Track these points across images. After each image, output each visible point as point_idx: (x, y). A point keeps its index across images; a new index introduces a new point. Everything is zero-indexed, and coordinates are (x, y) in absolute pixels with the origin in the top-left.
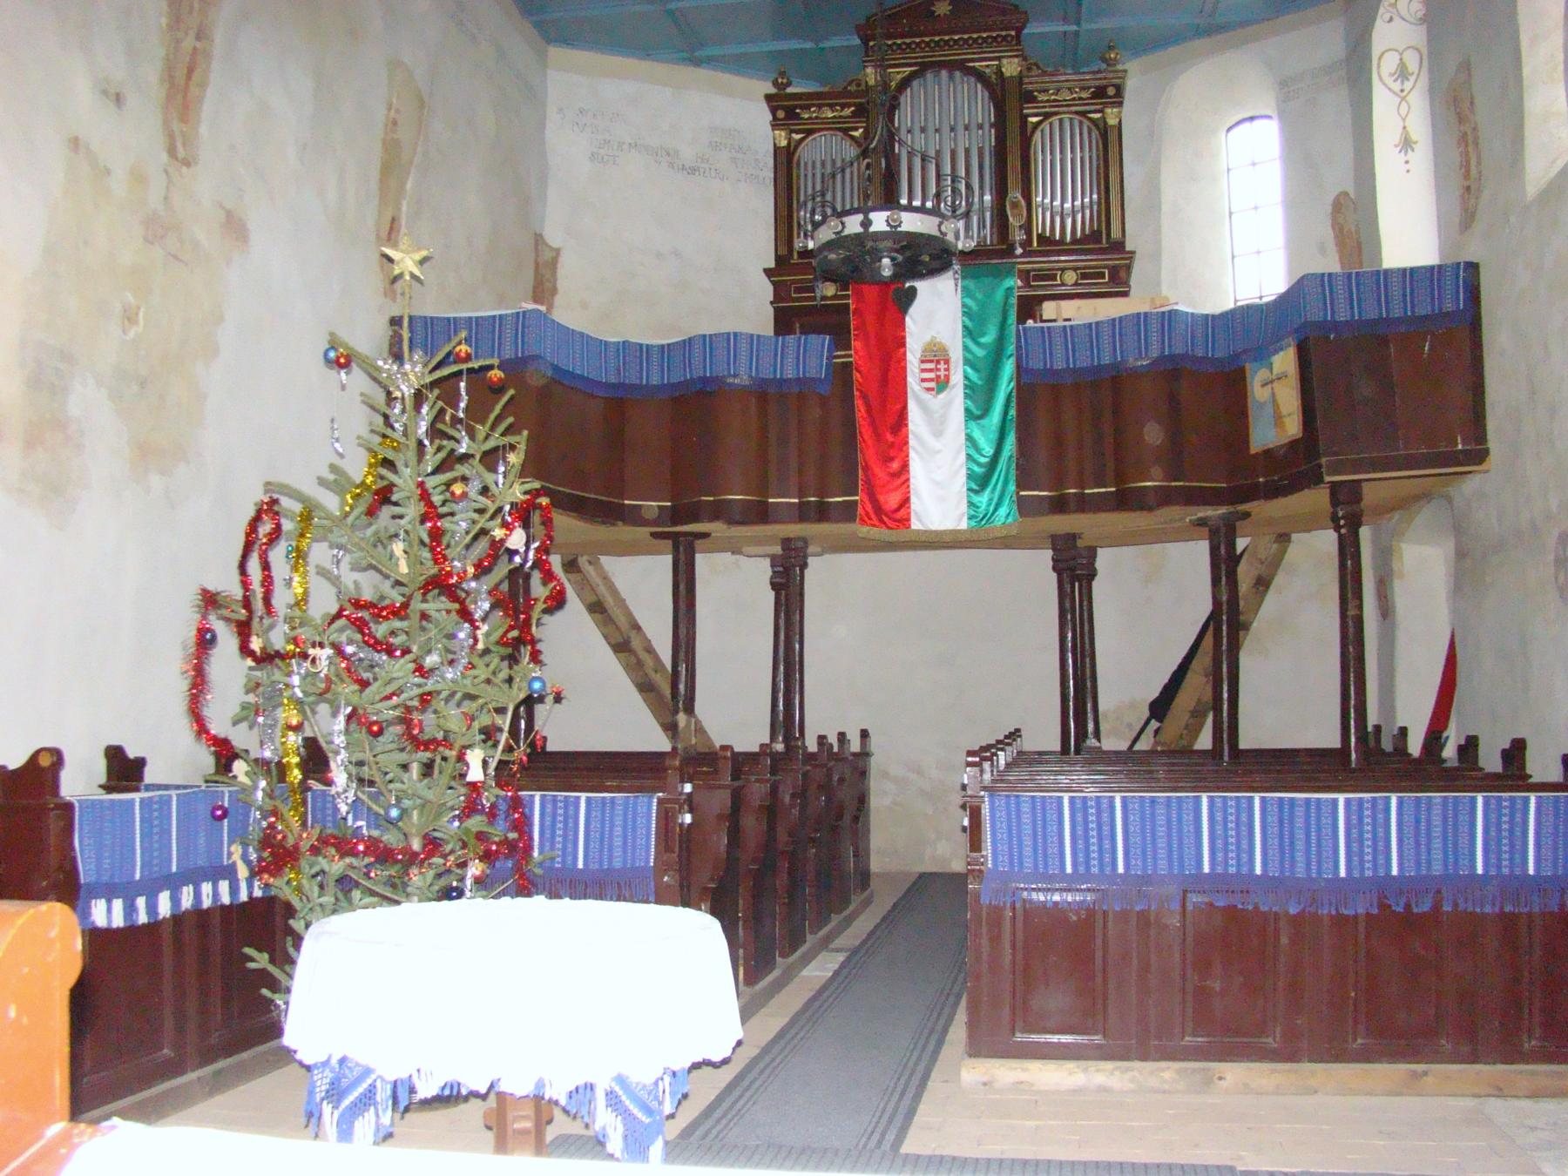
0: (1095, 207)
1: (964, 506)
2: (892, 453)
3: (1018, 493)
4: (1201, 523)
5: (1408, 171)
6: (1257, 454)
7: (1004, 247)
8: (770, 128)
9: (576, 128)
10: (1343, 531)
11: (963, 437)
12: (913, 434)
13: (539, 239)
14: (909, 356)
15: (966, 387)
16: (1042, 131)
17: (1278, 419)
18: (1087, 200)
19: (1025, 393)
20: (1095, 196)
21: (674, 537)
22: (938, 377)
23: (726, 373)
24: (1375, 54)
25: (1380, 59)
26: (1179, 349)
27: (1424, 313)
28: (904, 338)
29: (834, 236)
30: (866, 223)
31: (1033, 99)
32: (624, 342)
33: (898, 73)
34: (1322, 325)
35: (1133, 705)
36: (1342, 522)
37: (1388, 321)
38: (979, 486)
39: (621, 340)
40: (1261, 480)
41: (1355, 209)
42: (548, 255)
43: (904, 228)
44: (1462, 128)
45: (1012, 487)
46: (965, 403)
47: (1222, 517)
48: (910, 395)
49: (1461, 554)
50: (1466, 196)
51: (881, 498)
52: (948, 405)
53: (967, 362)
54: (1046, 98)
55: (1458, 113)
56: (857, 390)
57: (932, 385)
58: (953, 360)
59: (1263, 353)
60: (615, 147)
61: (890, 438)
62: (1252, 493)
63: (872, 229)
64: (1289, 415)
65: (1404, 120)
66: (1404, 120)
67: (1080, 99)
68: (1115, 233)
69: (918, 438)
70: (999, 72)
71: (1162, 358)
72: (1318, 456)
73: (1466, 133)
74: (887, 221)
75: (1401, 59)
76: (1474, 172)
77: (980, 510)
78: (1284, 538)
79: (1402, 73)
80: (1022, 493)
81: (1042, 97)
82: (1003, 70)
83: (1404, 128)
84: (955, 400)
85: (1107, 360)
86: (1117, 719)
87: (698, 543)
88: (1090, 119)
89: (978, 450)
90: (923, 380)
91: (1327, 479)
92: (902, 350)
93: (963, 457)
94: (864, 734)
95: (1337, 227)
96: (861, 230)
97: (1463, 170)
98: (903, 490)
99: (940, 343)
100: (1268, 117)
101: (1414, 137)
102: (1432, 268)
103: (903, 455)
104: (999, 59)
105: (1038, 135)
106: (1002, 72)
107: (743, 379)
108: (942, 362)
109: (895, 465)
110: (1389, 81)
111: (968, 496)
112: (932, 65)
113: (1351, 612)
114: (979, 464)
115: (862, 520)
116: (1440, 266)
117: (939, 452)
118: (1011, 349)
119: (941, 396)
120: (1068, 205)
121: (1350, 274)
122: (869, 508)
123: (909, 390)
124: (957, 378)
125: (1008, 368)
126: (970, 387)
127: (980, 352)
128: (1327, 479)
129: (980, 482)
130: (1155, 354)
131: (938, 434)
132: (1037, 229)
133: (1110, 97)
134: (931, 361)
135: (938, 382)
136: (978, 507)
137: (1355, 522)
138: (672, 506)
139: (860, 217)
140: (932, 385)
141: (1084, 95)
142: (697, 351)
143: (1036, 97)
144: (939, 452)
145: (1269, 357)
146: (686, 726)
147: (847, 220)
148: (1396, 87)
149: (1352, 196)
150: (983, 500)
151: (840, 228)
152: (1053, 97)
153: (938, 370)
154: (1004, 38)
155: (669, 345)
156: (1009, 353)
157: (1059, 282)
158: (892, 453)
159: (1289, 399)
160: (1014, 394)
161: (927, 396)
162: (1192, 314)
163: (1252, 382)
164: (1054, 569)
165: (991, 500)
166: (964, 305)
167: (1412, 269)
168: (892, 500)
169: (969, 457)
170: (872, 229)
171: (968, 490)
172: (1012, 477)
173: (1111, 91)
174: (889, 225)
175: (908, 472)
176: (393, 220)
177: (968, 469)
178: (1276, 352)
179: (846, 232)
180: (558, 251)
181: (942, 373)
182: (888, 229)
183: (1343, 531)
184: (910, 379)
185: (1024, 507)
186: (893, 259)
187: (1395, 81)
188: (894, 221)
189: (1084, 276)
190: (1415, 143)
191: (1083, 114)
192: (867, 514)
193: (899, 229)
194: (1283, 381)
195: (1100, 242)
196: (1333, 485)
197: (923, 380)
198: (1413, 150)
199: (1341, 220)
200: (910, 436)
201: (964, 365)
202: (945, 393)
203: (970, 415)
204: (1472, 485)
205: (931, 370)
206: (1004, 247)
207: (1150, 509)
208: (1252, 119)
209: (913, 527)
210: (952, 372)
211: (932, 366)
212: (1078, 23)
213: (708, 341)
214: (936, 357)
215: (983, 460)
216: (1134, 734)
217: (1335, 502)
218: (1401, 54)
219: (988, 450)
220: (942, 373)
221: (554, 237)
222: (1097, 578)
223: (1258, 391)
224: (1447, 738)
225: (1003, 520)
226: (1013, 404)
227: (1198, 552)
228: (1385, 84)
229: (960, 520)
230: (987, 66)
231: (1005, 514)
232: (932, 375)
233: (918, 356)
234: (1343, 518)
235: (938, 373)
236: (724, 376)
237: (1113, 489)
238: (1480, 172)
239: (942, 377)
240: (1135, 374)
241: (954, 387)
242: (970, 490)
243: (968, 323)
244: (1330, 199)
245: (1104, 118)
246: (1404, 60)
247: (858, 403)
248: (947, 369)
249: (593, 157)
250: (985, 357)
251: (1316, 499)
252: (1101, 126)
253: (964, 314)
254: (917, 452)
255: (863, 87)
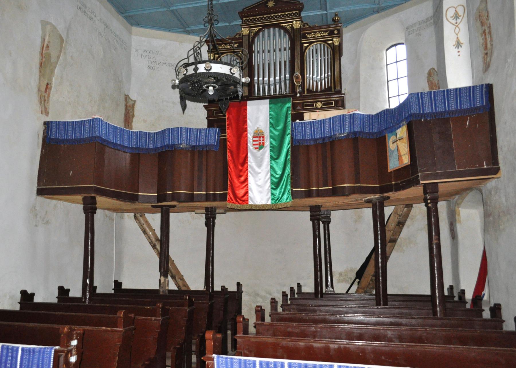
0: (330, 78)
1: (270, 195)
2: (241, 174)
3: (292, 190)
4: (369, 201)
5: (459, 55)
6: (391, 172)
7: (294, 94)
8: (207, 53)
9: (142, 56)
10: (430, 205)
11: (269, 167)
12: (250, 166)
13: (127, 97)
14: (249, 135)
15: (271, 147)
16: (309, 49)
17: (400, 156)
18: (326, 75)
19: (295, 148)
20: (329, 73)
21: (161, 207)
22: (260, 143)
23: (177, 143)
24: (445, 8)
25: (447, 11)
26: (357, 129)
27: (466, 107)
28: (247, 128)
29: (183, 76)
30: (196, 69)
31: (306, 37)
32: (140, 132)
33: (254, 30)
34: (420, 115)
35: (351, 270)
36: (429, 201)
37: (449, 112)
38: (275, 186)
39: (139, 131)
40: (393, 183)
41: (437, 75)
42: (131, 103)
43: (213, 71)
44: (483, 28)
45: (289, 187)
46: (270, 153)
47: (377, 199)
48: (248, 151)
49: (487, 215)
50: (486, 57)
51: (237, 192)
52: (263, 155)
53: (271, 137)
54: (310, 36)
55: (482, 22)
56: (228, 149)
57: (257, 146)
58: (265, 137)
59: (393, 129)
60: (157, 64)
61: (240, 168)
62: (389, 189)
63: (198, 72)
64: (404, 155)
65: (457, 35)
66: (457, 35)
67: (324, 36)
68: (338, 87)
69: (252, 168)
70: (292, 27)
71: (350, 134)
72: (418, 173)
73: (485, 30)
74: (205, 68)
75: (456, 10)
76: (489, 45)
77: (276, 196)
78: (409, 206)
79: (456, 16)
80: (294, 189)
81: (309, 36)
82: (294, 26)
83: (457, 38)
84: (267, 152)
85: (327, 135)
86: (346, 275)
87: (171, 210)
88: (328, 44)
89: (276, 172)
90: (254, 145)
91: (422, 182)
92: (246, 133)
93: (269, 175)
94: (239, 285)
95: (429, 82)
96: (194, 72)
97: (484, 45)
98: (245, 189)
99: (261, 130)
100: (403, 44)
101: (462, 41)
102: (470, 87)
103: (246, 174)
104: (292, 22)
105: (307, 51)
106: (293, 27)
107: (183, 146)
108: (261, 137)
109: (242, 179)
110: (451, 20)
111: (271, 191)
112: (268, 27)
113: (435, 242)
114: (276, 178)
115: (229, 200)
116: (473, 87)
117: (260, 173)
118: (289, 131)
119: (261, 151)
120: (319, 77)
121: (431, 92)
122: (232, 196)
123: (248, 149)
124: (267, 143)
125: (288, 139)
126: (272, 147)
127: (277, 133)
128: (422, 182)
129: (276, 185)
130: (347, 131)
131: (260, 166)
132: (306, 87)
133: (336, 34)
134: (257, 137)
135: (260, 146)
136: (275, 195)
137: (435, 201)
138: (157, 195)
139: (193, 67)
140: (257, 146)
141: (326, 34)
142: (166, 135)
143: (306, 36)
144: (260, 173)
145: (396, 130)
146: (164, 282)
147: (188, 68)
148: (454, 22)
149: (436, 69)
150: (277, 192)
151: (185, 72)
152: (313, 36)
153: (260, 140)
154: (294, 14)
155: (157, 133)
156: (288, 133)
157: (315, 107)
158: (241, 174)
159: (404, 148)
160: (290, 150)
161: (255, 151)
162: (363, 115)
163: (389, 141)
164: (311, 220)
165: (280, 192)
166: (270, 115)
167: (460, 89)
168: (241, 192)
169: (272, 175)
170: (198, 72)
171: (271, 188)
172: (289, 183)
173: (336, 32)
174: (206, 69)
175: (248, 181)
176: (48, 84)
177: (271, 180)
178: (398, 128)
179: (188, 74)
180: (135, 101)
181: (261, 142)
182: (205, 71)
183: (430, 205)
184: (248, 144)
185: (294, 195)
186: (214, 87)
187: (453, 19)
188: (208, 68)
189: (325, 104)
190: (462, 44)
191: (325, 41)
192: (231, 198)
193: (210, 71)
194: (402, 140)
195: (331, 90)
196: (425, 185)
197: (254, 145)
198: (461, 47)
199: (431, 79)
200: (249, 167)
201: (270, 138)
202: (262, 149)
203: (272, 158)
204: (491, 184)
205: (257, 141)
206: (294, 94)
207: (347, 196)
208: (396, 45)
209: (249, 203)
210: (265, 141)
211: (257, 139)
212: (326, 10)
213: (170, 131)
214: (259, 135)
215: (277, 176)
216: (352, 281)
217: (425, 193)
218: (456, 8)
219: (280, 172)
220: (261, 142)
221: (133, 96)
222: (331, 223)
223: (391, 146)
224: (484, 295)
225: (285, 200)
226: (290, 153)
227: (368, 213)
228: (449, 21)
229: (268, 201)
230: (288, 25)
231: (287, 198)
232: (257, 143)
233: (252, 135)
234: (429, 199)
235: (260, 142)
236: (176, 144)
237: (331, 188)
238: (492, 45)
239: (262, 143)
240: (340, 140)
241: (266, 146)
242: (272, 188)
243: (272, 122)
244: (427, 71)
245: (333, 43)
246: (457, 11)
247: (229, 154)
248: (263, 140)
249: (149, 67)
250: (277, 135)
251: (417, 191)
252: (332, 46)
253: (270, 118)
254: (251, 173)
255: (241, 36)
